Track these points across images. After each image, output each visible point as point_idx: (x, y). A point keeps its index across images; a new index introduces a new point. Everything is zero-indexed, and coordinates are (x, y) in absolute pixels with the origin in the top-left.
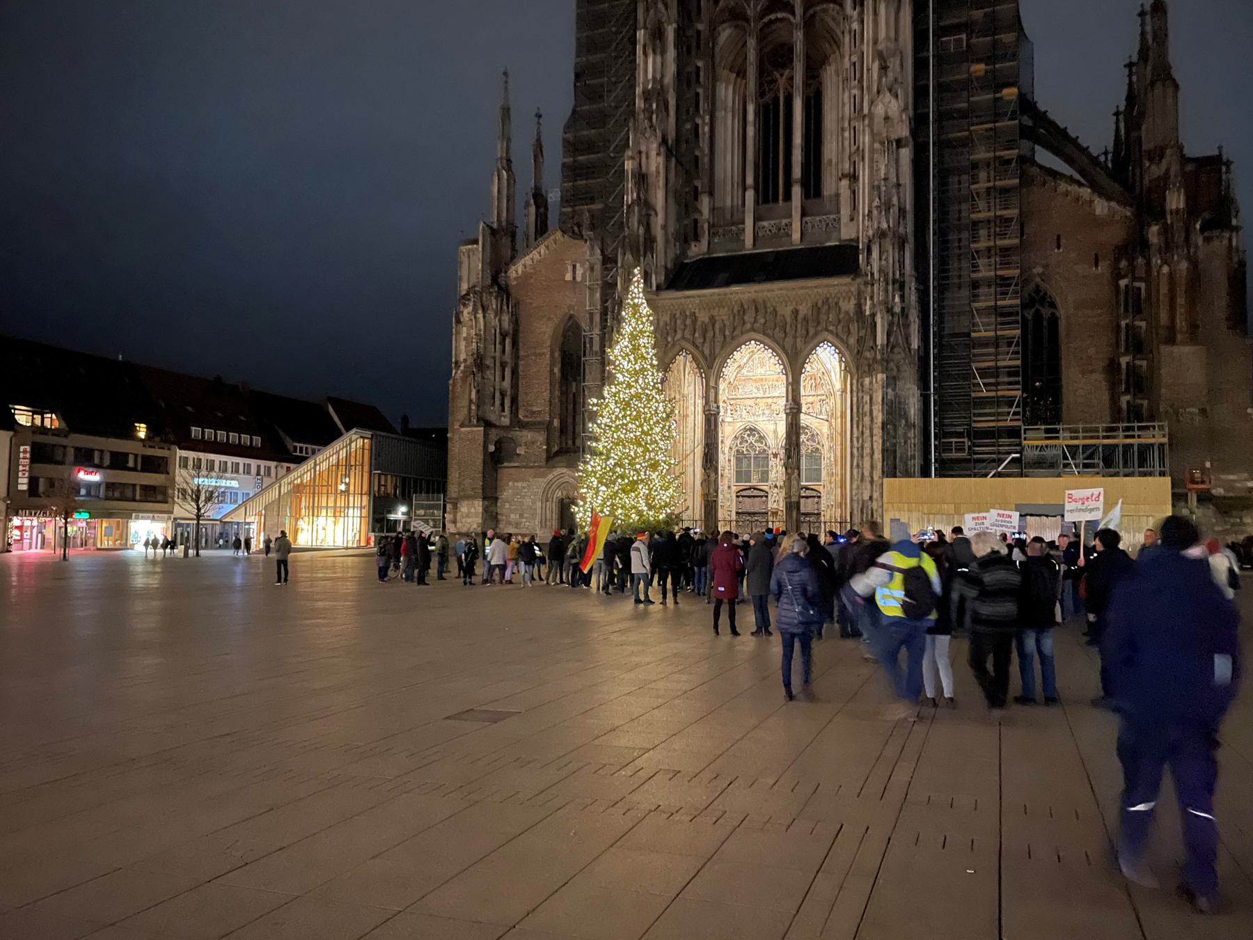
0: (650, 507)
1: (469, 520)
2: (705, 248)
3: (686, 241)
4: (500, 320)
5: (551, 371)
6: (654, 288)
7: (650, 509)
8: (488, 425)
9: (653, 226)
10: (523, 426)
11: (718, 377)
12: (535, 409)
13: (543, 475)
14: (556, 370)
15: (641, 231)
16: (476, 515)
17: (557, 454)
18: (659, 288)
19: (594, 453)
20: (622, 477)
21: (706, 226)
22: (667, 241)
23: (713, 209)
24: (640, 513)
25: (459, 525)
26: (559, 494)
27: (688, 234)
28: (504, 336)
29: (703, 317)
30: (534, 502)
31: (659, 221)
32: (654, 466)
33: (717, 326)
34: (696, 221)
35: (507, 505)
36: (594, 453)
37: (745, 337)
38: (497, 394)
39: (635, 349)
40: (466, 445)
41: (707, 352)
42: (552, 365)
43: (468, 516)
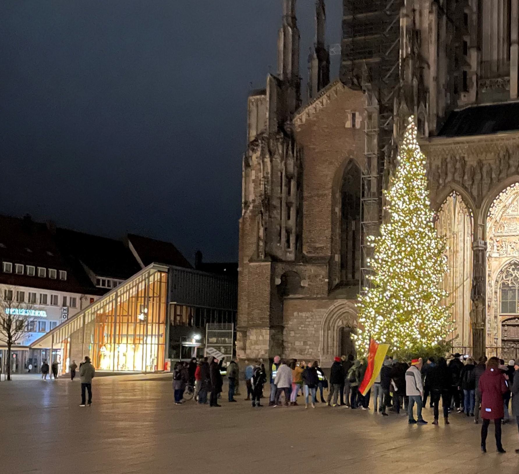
0: (423, 335)
1: (257, 347)
2: (473, 99)
3: (456, 92)
4: (286, 164)
5: (333, 212)
6: (427, 134)
7: (423, 337)
8: (275, 260)
9: (425, 78)
10: (307, 261)
11: (485, 216)
12: (318, 245)
13: (325, 306)
14: (337, 210)
15: (415, 82)
16: (264, 342)
17: (338, 286)
18: (431, 134)
19: (372, 285)
20: (398, 308)
21: (474, 78)
22: (438, 92)
23: (481, 63)
24: (414, 341)
25: (248, 351)
26: (339, 323)
27: (458, 85)
28: (289, 178)
29: (471, 161)
30: (317, 331)
31: (431, 73)
32: (427, 298)
33: (485, 170)
34: (465, 73)
35: (292, 334)
36: (372, 285)
37: (511, 179)
38: (283, 232)
39: (410, 190)
40: (254, 278)
41: (475, 193)
42: (333, 206)
43: (256, 343)
